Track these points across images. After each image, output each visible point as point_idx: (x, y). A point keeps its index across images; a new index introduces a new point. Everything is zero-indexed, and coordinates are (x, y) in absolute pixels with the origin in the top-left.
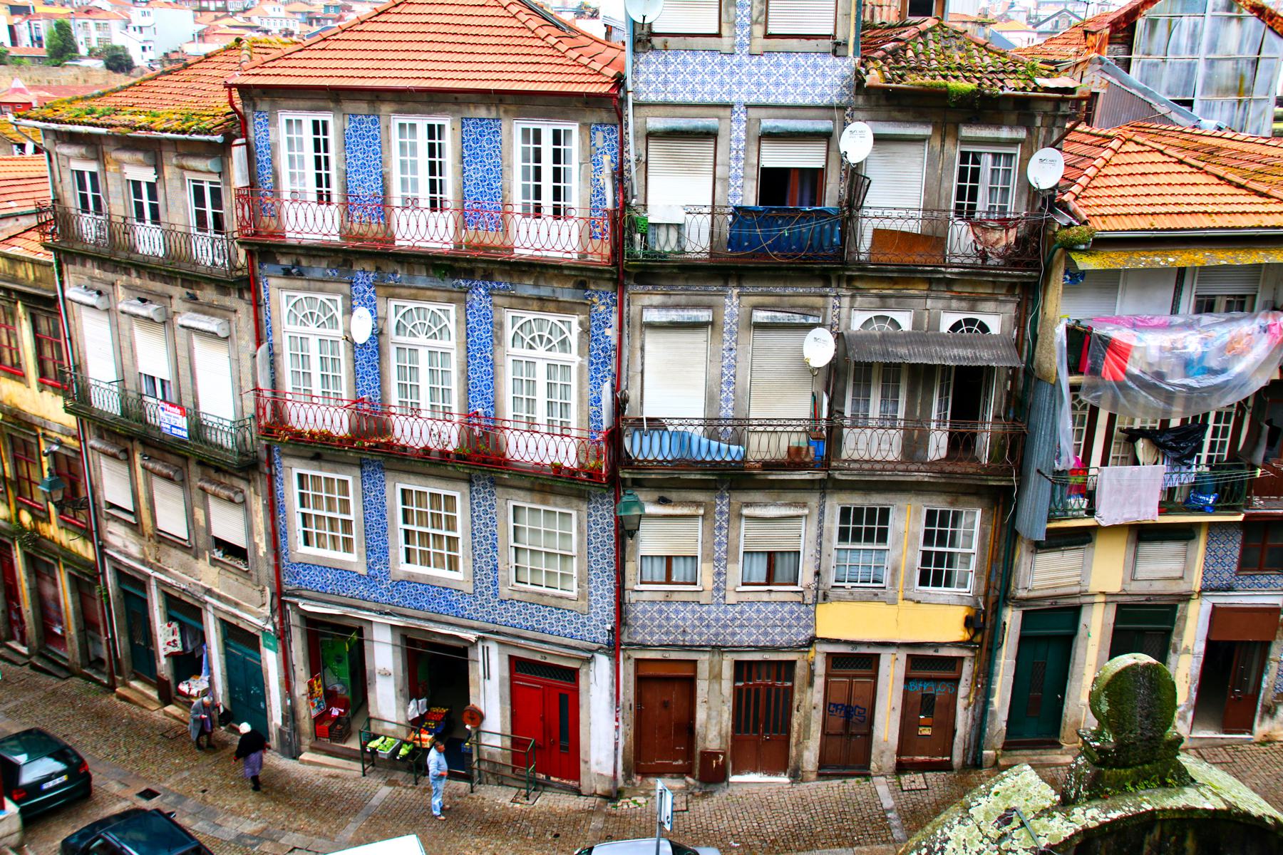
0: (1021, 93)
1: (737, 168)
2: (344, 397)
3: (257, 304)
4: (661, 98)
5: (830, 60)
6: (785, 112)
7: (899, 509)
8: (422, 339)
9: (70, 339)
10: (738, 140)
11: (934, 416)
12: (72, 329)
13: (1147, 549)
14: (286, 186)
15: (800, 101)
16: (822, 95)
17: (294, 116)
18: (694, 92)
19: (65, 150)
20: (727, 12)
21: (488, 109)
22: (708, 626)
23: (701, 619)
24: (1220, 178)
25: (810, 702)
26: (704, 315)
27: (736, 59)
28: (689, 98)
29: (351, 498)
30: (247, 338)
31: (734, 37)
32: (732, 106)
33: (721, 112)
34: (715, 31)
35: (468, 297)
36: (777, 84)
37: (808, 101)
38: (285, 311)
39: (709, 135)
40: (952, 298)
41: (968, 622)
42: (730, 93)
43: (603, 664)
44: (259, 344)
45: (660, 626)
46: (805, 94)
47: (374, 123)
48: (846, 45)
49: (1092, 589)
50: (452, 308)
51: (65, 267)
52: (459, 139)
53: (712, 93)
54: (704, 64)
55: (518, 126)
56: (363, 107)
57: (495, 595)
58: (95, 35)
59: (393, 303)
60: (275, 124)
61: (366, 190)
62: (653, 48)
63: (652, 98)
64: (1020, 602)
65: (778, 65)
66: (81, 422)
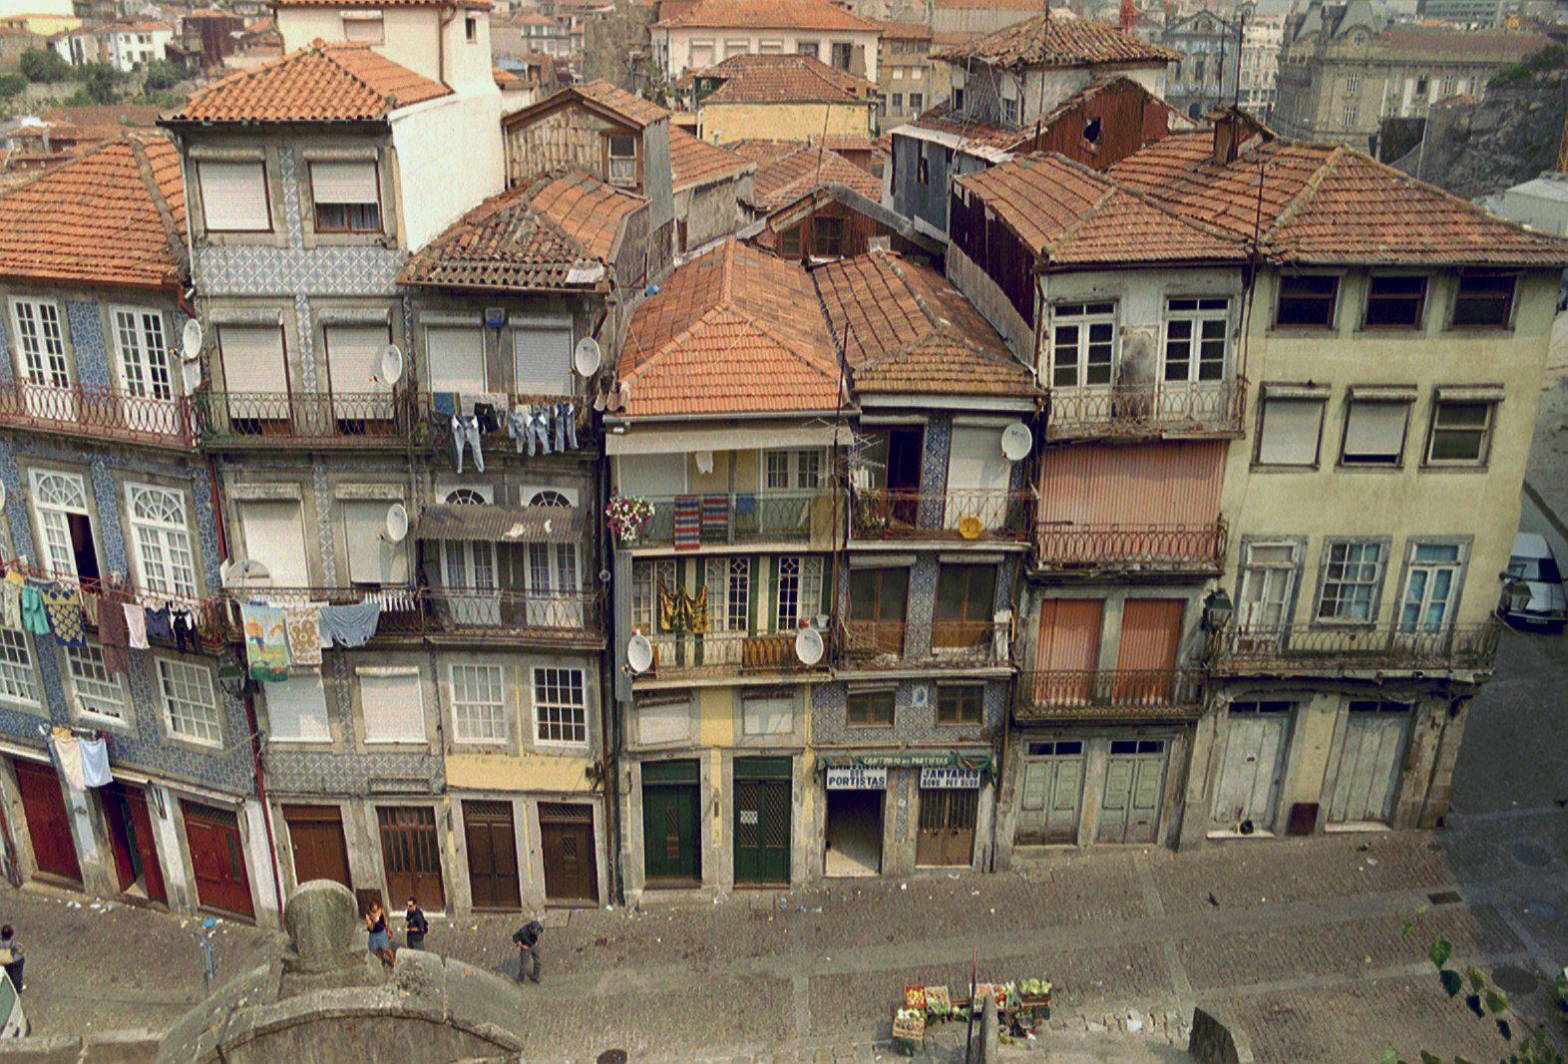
0: (543, 288)
4: (225, 290)
5: (382, 252)
6: (345, 302)
7: (506, 670)
11: (528, 585)
13: (750, 705)
15: (359, 291)
16: (379, 285)
18: (256, 284)
22: (344, 774)
23: (336, 767)
24: (793, 353)
25: (453, 847)
26: (289, 490)
28: (252, 290)
29: (27, 649)
31: (287, 231)
33: (284, 303)
34: (267, 227)
39: (271, 326)
40: (527, 473)
41: (588, 772)
42: (291, 284)
43: (253, 813)
45: (300, 774)
48: (394, 238)
49: (704, 742)
50: (80, 478)
54: (262, 258)
55: (114, 311)
57: (158, 743)
58: (136, 47)
62: (211, 244)
63: (217, 290)
64: (634, 755)
65: (333, 258)
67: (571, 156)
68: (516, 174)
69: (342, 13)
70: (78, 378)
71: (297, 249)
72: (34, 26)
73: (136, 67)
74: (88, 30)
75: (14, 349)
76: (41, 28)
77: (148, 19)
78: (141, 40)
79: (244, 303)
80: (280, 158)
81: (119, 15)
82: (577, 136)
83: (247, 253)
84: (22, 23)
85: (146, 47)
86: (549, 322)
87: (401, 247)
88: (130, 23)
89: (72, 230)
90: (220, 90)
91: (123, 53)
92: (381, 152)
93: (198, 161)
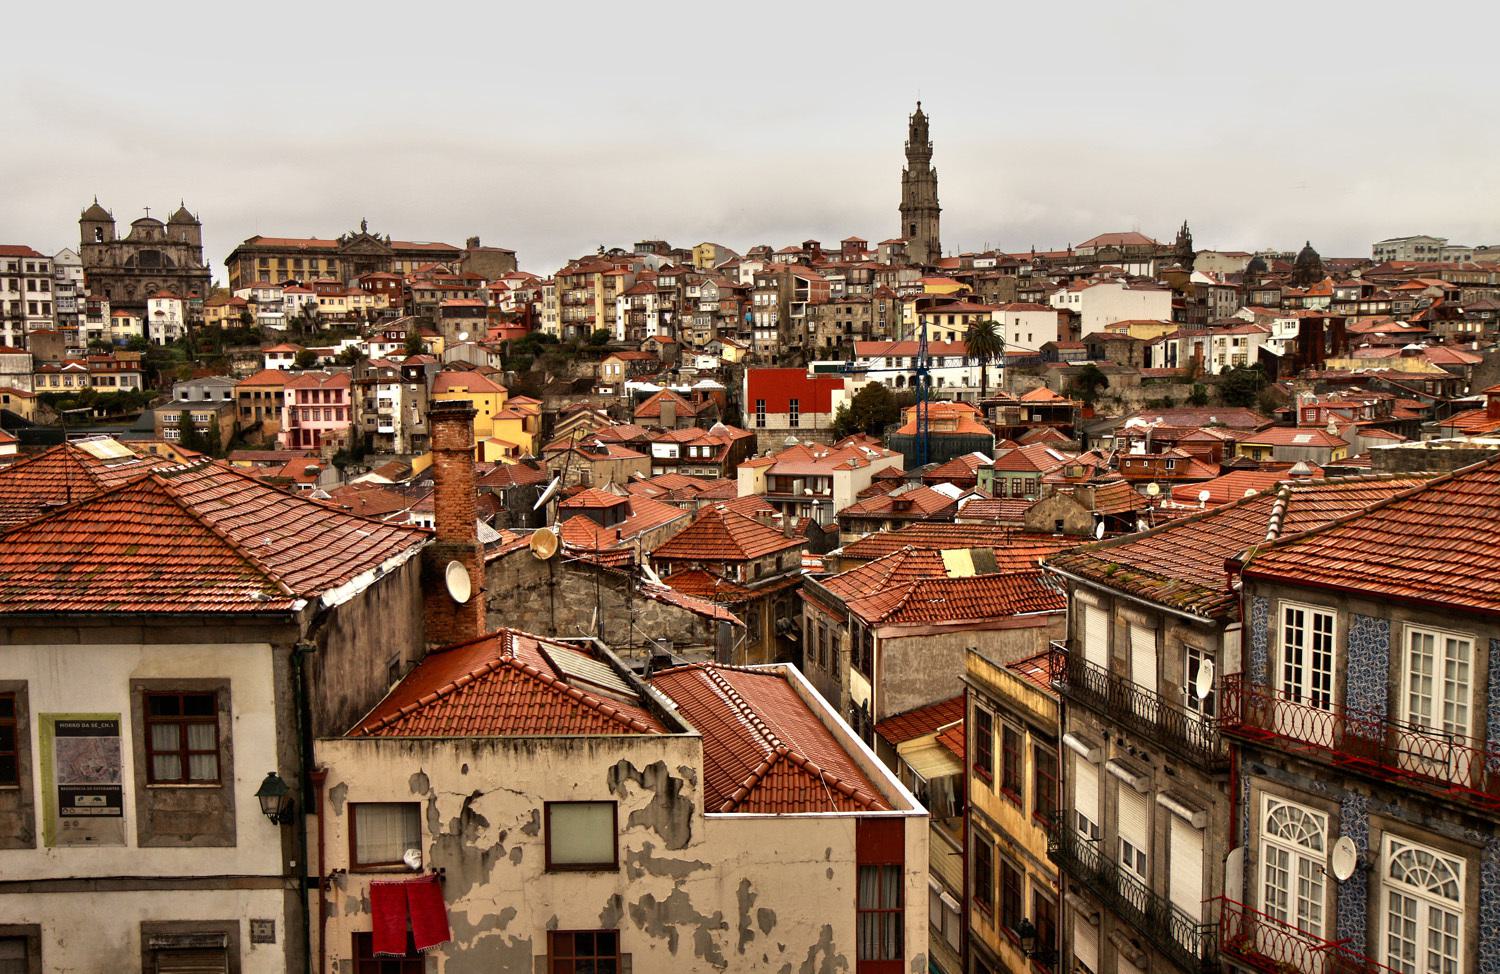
2: (1323, 937)
3: (1236, 802)
8: (1422, 890)
9: (1063, 782)
12: (1067, 772)
14: (1280, 682)
19: (1079, 595)
30: (1223, 835)
35: (1484, 854)
38: (1265, 816)
44: (1234, 845)
51: (1068, 709)
52: (1484, 663)
56: (1372, 610)
58: (1232, 350)
59: (1388, 839)
60: (1272, 610)
61: (1367, 700)
66: (1062, 873)
72: (1135, 332)
73: (1225, 370)
74: (1185, 335)
75: (1397, 686)
76: (1144, 334)
77: (1242, 322)
78: (1236, 342)
81: (1210, 320)
85: (1236, 350)
88: (1228, 327)
91: (1215, 355)
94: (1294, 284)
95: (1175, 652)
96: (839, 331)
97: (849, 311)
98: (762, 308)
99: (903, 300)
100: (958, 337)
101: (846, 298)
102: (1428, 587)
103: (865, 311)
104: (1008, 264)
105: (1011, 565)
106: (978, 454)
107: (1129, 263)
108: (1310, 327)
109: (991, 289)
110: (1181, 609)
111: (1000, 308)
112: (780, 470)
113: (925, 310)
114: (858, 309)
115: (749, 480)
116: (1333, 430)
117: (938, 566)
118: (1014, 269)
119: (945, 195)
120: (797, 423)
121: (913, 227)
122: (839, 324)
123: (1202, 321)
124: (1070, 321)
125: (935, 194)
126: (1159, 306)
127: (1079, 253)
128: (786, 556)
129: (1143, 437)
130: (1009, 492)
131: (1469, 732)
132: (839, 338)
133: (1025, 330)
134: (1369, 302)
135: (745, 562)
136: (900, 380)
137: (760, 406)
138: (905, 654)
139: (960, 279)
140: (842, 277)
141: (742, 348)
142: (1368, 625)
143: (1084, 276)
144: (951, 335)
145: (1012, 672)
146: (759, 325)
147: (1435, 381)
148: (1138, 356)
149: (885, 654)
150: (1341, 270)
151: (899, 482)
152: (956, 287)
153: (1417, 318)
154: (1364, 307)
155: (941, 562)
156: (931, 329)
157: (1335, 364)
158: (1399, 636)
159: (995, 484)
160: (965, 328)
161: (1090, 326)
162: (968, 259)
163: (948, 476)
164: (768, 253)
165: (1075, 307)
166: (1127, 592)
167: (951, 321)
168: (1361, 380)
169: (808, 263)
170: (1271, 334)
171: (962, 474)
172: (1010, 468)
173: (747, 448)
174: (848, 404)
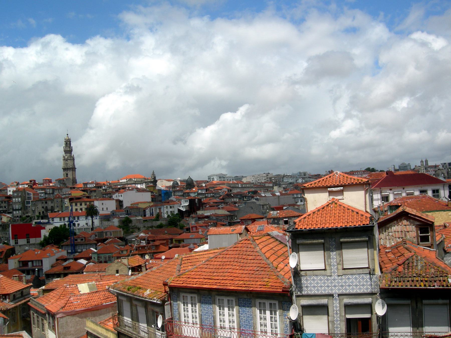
0: (441, 287)
1: (337, 317)
10: (336, 307)
14: (183, 319)
16: (367, 289)
17: (185, 295)
18: (318, 290)
19: (120, 297)
20: (328, 261)
21: (247, 295)
27: (333, 278)
28: (316, 292)
31: (331, 270)
32: (332, 295)
34: (324, 268)
36: (349, 286)
37: (361, 291)
42: (332, 290)
46: (360, 289)
47: (210, 298)
53: (325, 290)
54: (321, 280)
55: (258, 301)
60: (178, 296)
67: (404, 236)
68: (382, 243)
69: (329, 189)
70: (240, 327)
71: (335, 276)
72: (141, 206)
73: (168, 216)
74: (155, 206)
78: (171, 207)
79: (313, 298)
80: (330, 241)
82: (406, 228)
83: (315, 278)
84: (138, 203)
85: (171, 210)
86: (440, 301)
87: (376, 274)
88: (168, 203)
89: (237, 271)
90: (305, 218)
91: (165, 212)
92: (369, 238)
93: (298, 245)
94: (187, 189)
95: (151, 313)
96: (43, 210)
97: (46, 203)
98: (15, 203)
99: (64, 198)
100: (84, 210)
101: (45, 198)
102: (221, 284)
103: (52, 202)
104: (98, 186)
105: (101, 287)
106: (92, 249)
107: (137, 184)
108: (192, 202)
109: (94, 194)
110: (151, 299)
111: (97, 200)
112: (22, 260)
113: (72, 201)
114: (49, 203)
115: (13, 263)
116: (200, 233)
117: (76, 290)
118: (101, 187)
119: (78, 163)
120: (29, 242)
121: (67, 174)
122: (43, 207)
123: (161, 201)
124: (120, 203)
125: (74, 163)
126: (147, 197)
127: (121, 181)
128: (24, 291)
129: (144, 240)
130: (103, 261)
131: (236, 327)
132: (43, 212)
133: (105, 206)
134: (208, 193)
135: (8, 295)
136: (65, 224)
137: (16, 237)
138: (67, 322)
139: (83, 191)
140: (43, 191)
141: (9, 217)
142: (206, 298)
143: (123, 188)
144: (81, 209)
145: (102, 325)
146: (15, 209)
147: (227, 216)
148: (142, 213)
149: (59, 323)
150: (199, 183)
151: (65, 260)
152: (82, 193)
153: (221, 197)
154: (207, 195)
155: (77, 288)
156: (74, 208)
157: (200, 213)
158: (214, 300)
159: (98, 257)
160: (86, 207)
161: (126, 204)
162: (85, 184)
163: (83, 256)
164: (18, 184)
165: (121, 199)
166: (135, 295)
167: (81, 205)
168: (207, 217)
169: (31, 187)
170: (181, 204)
171: (87, 256)
172: (103, 252)
173: (12, 252)
174: (47, 234)
